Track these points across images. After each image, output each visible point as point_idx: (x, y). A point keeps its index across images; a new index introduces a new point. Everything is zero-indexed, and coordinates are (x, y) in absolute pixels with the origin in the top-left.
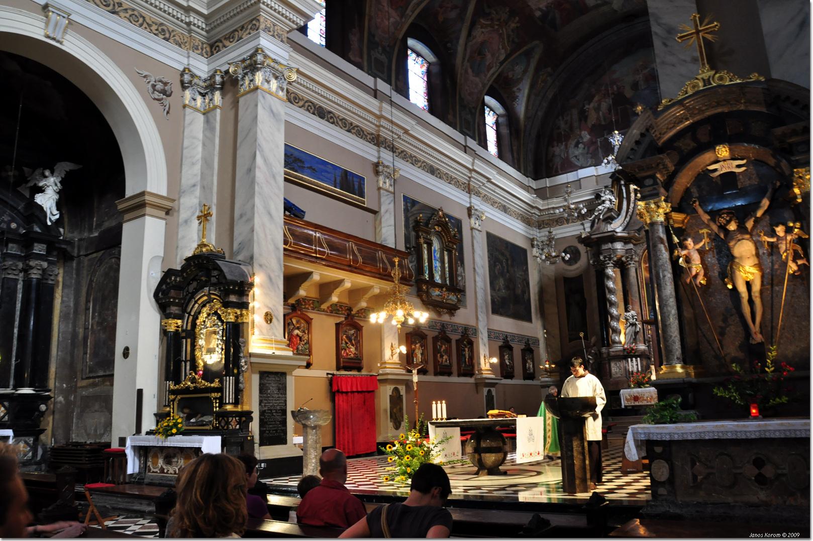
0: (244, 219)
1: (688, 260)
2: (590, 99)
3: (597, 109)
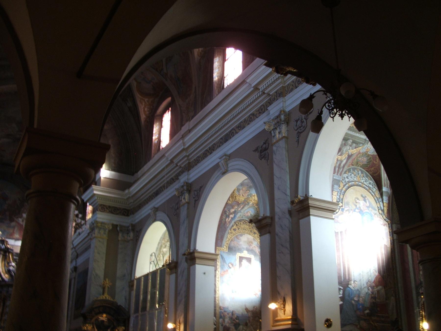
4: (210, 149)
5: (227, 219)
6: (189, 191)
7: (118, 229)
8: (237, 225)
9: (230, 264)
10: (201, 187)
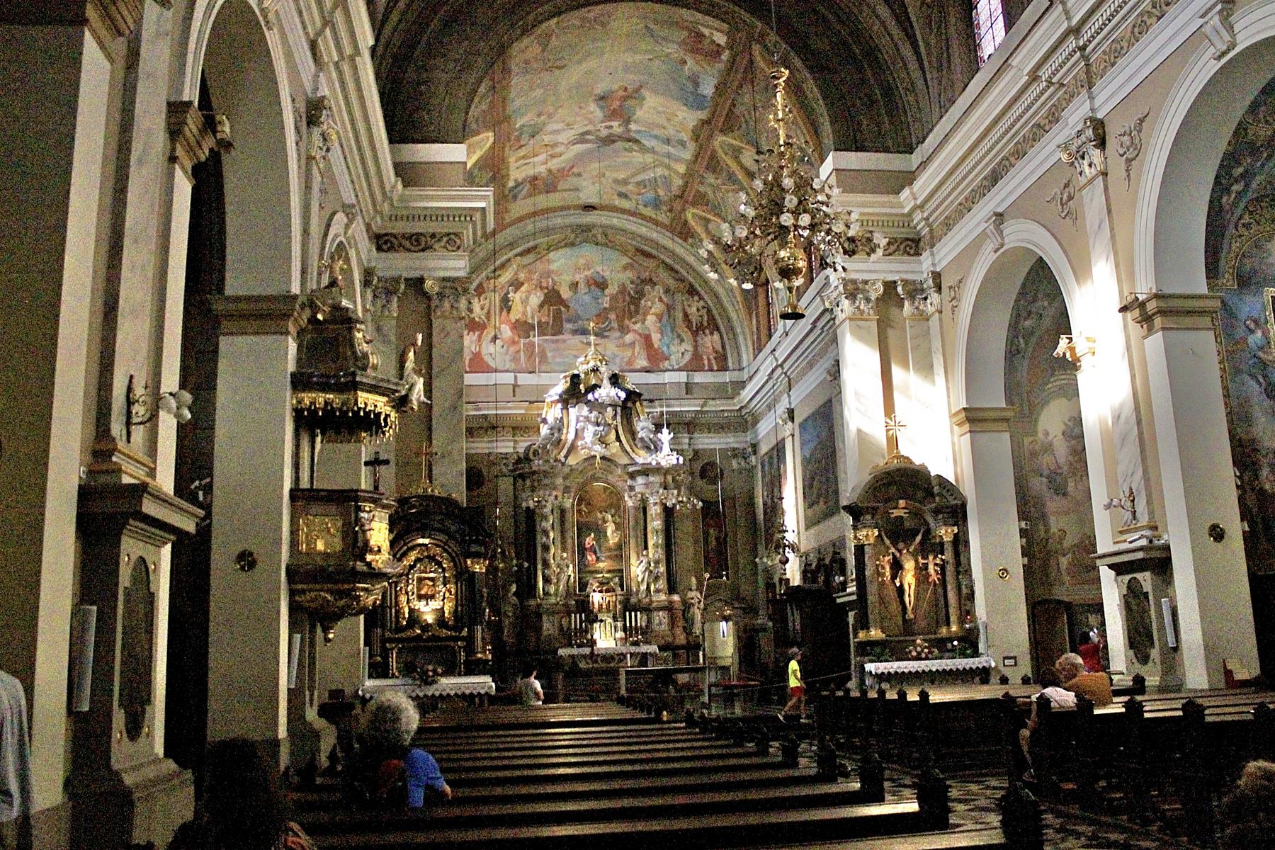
0: (446, 461)
1: (883, 568)
2: (517, 285)
3: (525, 302)
4: (1154, 7)
5: (1224, 200)
6: (1101, 143)
7: (900, 289)
8: (1251, 213)
9: (1248, 322)
10: (1142, 120)
